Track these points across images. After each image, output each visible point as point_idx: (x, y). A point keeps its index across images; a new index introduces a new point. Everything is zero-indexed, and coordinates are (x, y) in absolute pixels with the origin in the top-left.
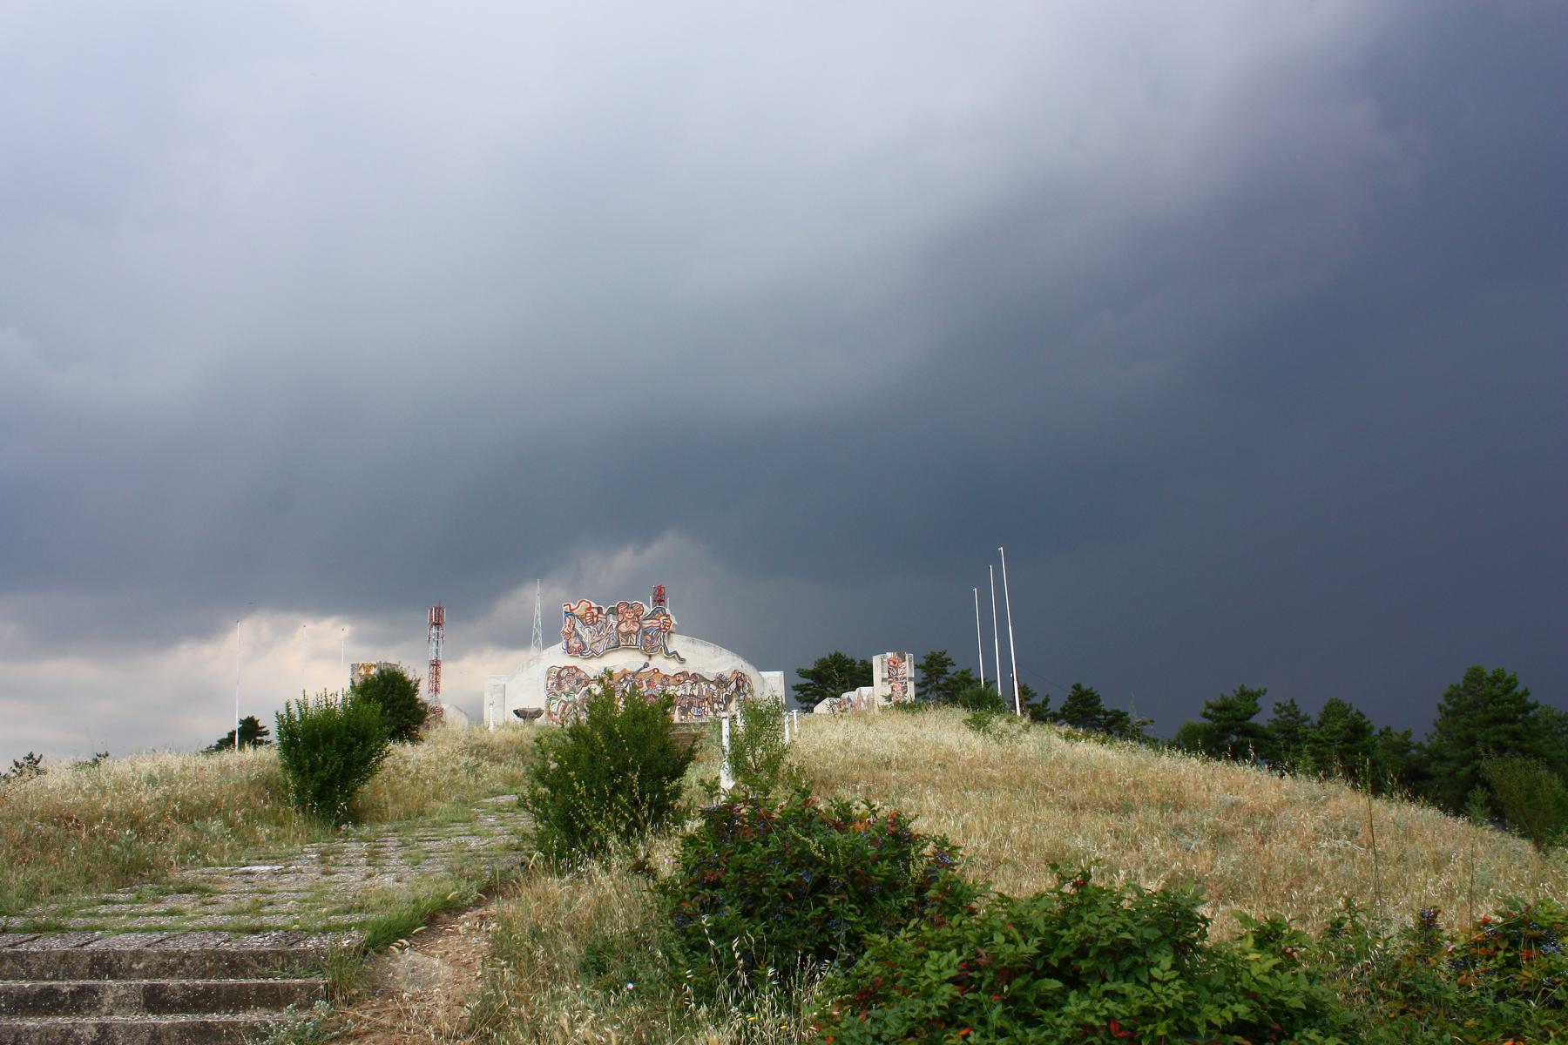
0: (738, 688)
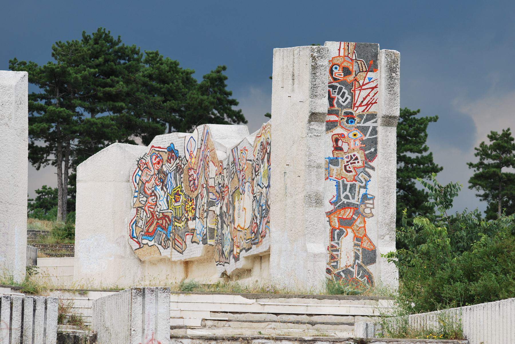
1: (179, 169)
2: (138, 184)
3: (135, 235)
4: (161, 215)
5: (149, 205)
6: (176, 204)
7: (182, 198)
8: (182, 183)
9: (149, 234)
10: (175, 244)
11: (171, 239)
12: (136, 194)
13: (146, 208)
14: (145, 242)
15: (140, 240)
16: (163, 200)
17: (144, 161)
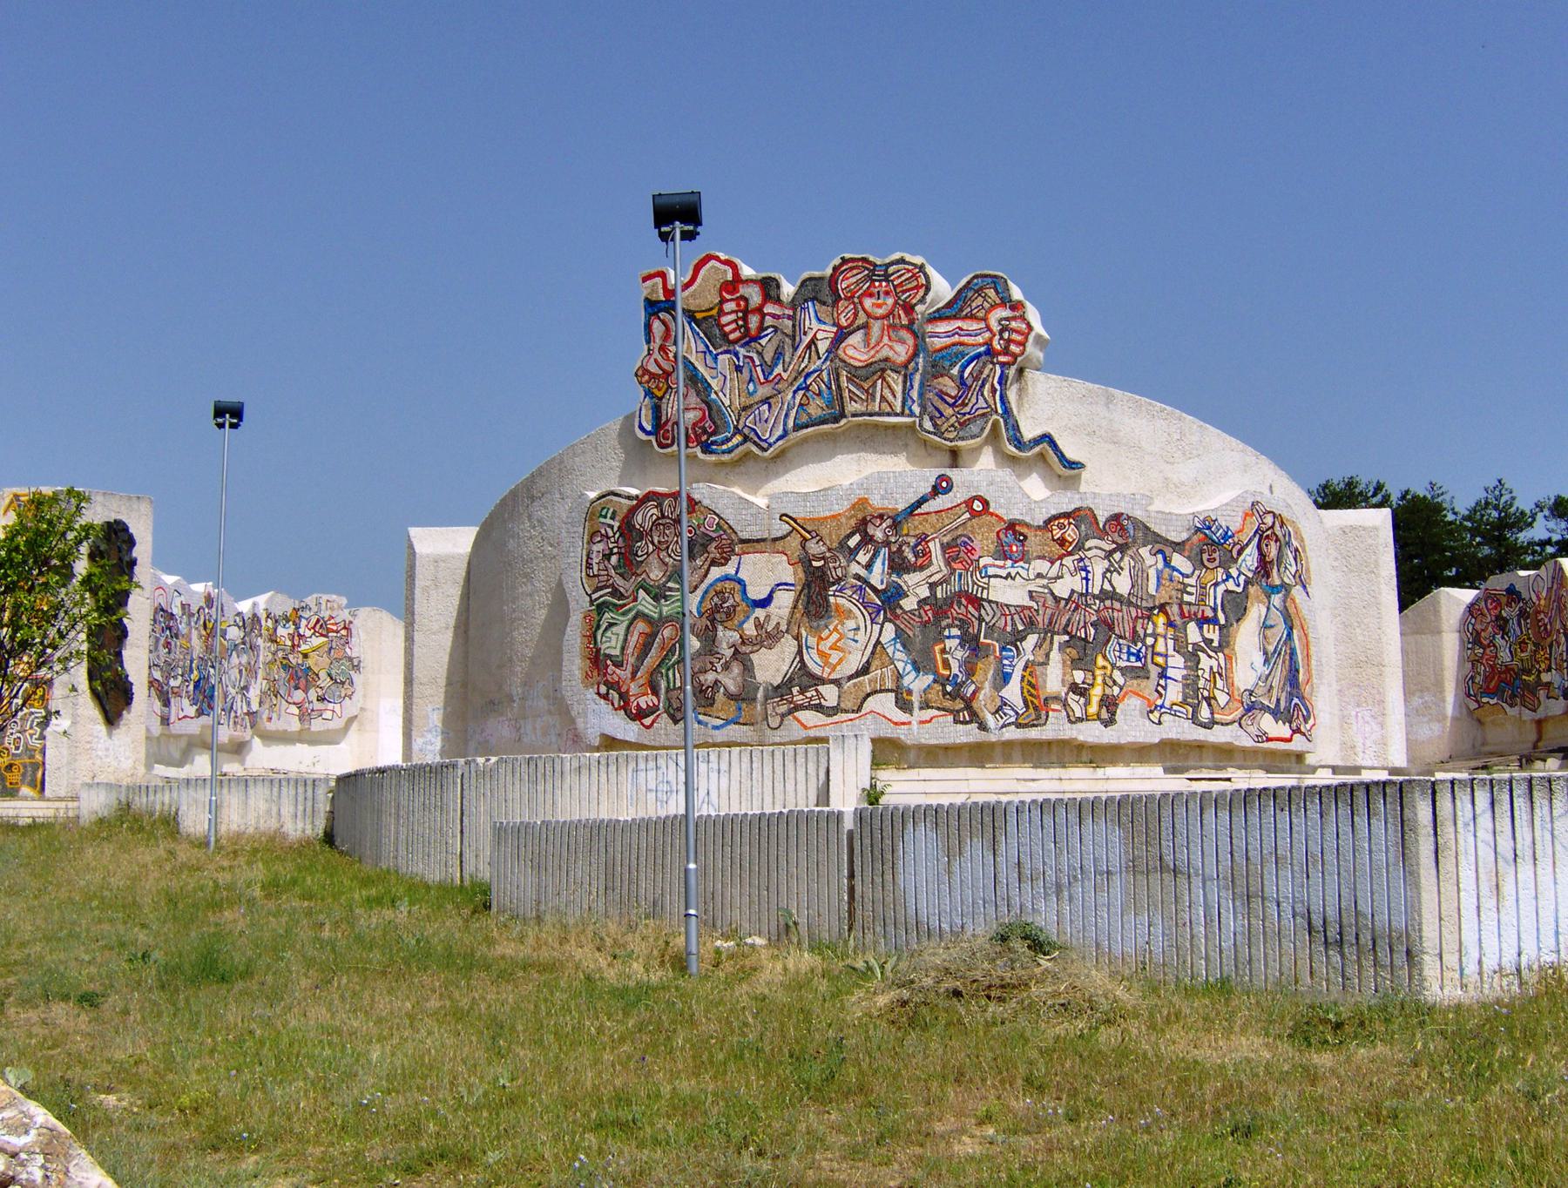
0: (1264, 567)
1: (1523, 614)
7: (1530, 647)
9: (1489, 692)
14: (1485, 700)
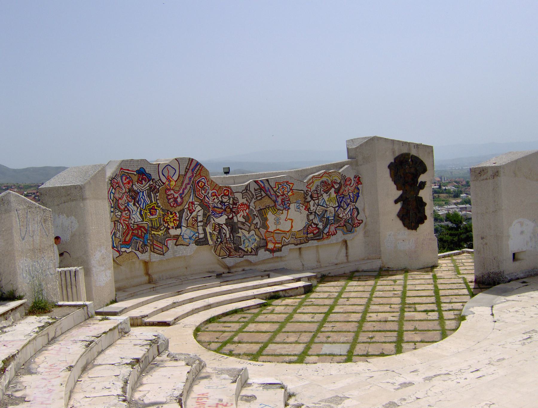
1: (152, 189)
2: (113, 201)
3: (115, 245)
4: (136, 226)
5: (123, 218)
6: (151, 217)
7: (159, 212)
8: (157, 200)
9: (126, 244)
10: (154, 248)
11: (149, 245)
12: (112, 210)
13: (122, 221)
14: (123, 250)
15: (119, 249)
16: (136, 214)
17: (116, 181)
